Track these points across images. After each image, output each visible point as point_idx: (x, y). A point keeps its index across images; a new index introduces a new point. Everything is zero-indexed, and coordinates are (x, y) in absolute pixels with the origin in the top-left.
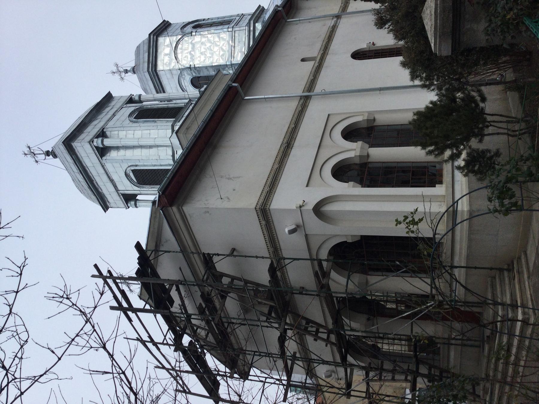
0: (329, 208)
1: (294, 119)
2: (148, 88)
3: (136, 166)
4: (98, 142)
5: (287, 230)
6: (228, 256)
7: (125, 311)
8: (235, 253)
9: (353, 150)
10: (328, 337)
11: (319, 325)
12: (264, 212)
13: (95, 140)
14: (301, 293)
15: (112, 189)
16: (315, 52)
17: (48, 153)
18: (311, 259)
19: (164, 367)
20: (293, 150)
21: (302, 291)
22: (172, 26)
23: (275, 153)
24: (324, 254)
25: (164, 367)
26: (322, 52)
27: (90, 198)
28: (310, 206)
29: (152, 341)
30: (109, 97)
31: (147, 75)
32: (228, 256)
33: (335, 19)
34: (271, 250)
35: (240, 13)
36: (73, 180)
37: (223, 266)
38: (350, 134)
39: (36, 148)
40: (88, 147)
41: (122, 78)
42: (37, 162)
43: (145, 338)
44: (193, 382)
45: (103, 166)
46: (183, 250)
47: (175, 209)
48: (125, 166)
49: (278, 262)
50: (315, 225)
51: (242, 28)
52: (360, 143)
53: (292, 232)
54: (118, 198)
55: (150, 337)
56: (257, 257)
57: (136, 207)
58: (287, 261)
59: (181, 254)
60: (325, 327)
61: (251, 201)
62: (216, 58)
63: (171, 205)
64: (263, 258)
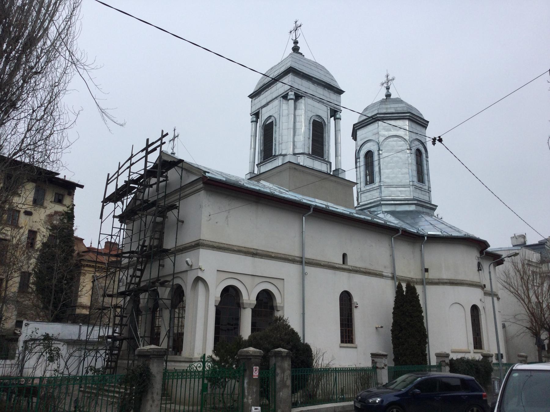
1: (279, 256)
3: (276, 125)
4: (291, 95)
5: (188, 259)
6: (178, 219)
7: (146, 149)
8: (180, 223)
9: (249, 297)
10: (133, 284)
11: (140, 277)
12: (197, 245)
13: (293, 93)
14: (160, 265)
15: (264, 103)
17: (296, 42)
18: (174, 274)
19: (119, 169)
20: (251, 258)
21: (162, 266)
22: (423, 130)
24: (177, 281)
25: (119, 169)
26: (351, 268)
27: (258, 84)
28: (200, 274)
29: (131, 165)
30: (340, 92)
32: (178, 219)
33: (390, 275)
34: (181, 248)
35: (432, 189)
36: (272, 68)
37: (172, 215)
41: (383, 84)
42: (291, 32)
43: (134, 160)
44: (111, 189)
45: (276, 98)
46: (182, 188)
47: (202, 185)
48: (276, 116)
49: (172, 253)
50: (191, 277)
51: (412, 193)
52: (255, 302)
54: (257, 108)
55: (133, 164)
56: (176, 239)
57: (252, 122)
58: (173, 258)
59: (179, 187)
60: (140, 281)
61: (206, 235)
62: (387, 171)
63: (203, 183)
64: (176, 242)
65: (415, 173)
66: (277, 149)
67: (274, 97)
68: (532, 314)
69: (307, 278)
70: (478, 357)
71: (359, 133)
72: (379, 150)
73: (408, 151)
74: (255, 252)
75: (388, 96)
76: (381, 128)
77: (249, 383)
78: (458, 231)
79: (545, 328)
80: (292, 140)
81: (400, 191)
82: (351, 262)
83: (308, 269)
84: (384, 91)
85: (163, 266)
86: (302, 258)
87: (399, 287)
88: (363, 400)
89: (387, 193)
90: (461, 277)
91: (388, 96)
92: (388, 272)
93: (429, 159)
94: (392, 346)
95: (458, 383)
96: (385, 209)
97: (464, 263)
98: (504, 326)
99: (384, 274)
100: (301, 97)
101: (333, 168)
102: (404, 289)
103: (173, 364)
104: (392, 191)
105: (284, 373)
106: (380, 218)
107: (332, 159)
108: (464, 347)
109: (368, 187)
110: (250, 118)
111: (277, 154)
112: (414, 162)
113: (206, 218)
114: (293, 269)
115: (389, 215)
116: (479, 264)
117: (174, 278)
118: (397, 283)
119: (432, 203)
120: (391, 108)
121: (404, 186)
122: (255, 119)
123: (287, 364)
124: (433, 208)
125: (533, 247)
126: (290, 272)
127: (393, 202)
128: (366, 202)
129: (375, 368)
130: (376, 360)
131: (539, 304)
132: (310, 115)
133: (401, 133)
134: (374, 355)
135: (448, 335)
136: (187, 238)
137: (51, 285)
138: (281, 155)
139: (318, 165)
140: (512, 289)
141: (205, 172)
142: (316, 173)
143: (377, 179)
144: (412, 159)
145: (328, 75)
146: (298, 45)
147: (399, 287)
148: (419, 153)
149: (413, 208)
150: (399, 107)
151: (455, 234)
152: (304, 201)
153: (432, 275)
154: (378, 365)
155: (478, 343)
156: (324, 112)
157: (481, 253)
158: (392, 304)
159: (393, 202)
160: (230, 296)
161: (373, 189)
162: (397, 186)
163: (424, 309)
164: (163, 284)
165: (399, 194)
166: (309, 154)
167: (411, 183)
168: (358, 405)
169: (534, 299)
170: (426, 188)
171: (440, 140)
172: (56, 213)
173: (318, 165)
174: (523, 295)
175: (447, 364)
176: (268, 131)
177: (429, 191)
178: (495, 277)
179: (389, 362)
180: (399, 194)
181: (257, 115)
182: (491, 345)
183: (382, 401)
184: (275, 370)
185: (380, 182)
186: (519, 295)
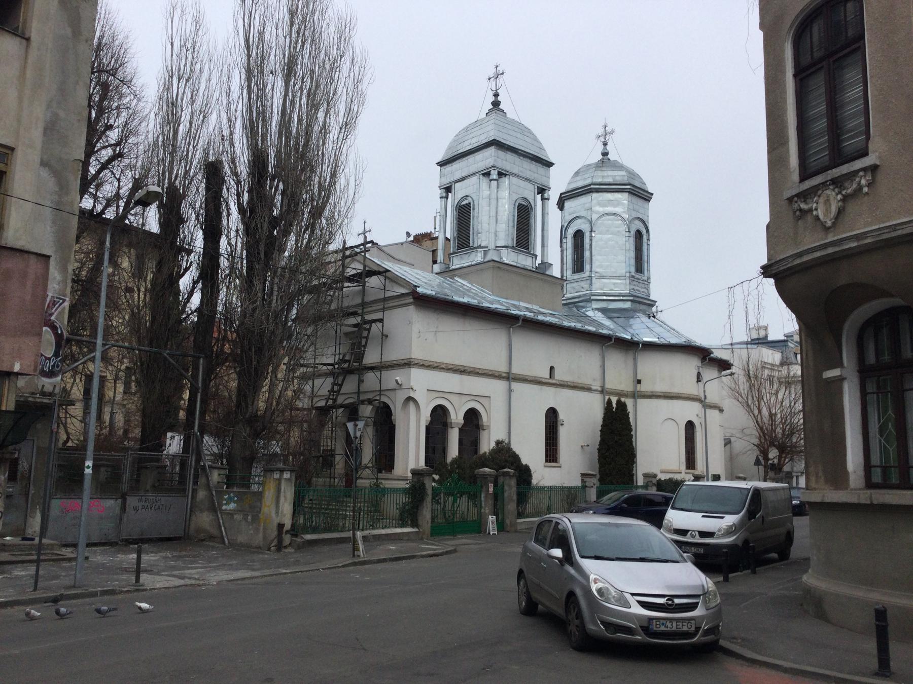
0: (412, 405)
2: (578, 178)
6: (383, 334)
9: (457, 417)
12: (408, 364)
16: (559, 376)
21: (361, 381)
22: (645, 203)
27: (449, 148)
30: (549, 164)
31: (588, 182)
33: (599, 389)
35: (652, 280)
36: (467, 129)
37: (375, 327)
40: (489, 162)
45: (474, 174)
46: (385, 299)
47: (412, 300)
50: (401, 396)
53: (397, 381)
54: (449, 181)
61: (417, 354)
62: (599, 257)
65: (633, 262)
66: (475, 241)
67: (472, 171)
68: (761, 428)
69: (513, 394)
71: (567, 204)
73: (627, 234)
74: (462, 369)
75: (605, 154)
76: (594, 202)
77: (486, 497)
79: (774, 446)
80: (493, 226)
81: (614, 284)
82: (559, 376)
83: (515, 386)
84: (600, 148)
87: (609, 402)
89: (599, 286)
90: (675, 390)
91: (605, 154)
92: (596, 386)
93: (651, 242)
94: (598, 465)
96: (595, 305)
97: (680, 373)
98: (728, 442)
99: (593, 387)
100: (506, 175)
101: (539, 261)
102: (614, 405)
105: (511, 489)
106: (593, 322)
107: (538, 251)
108: (674, 467)
109: (576, 276)
110: (438, 192)
111: (476, 245)
112: (633, 248)
113: (416, 335)
115: (600, 314)
116: (699, 375)
117: (380, 395)
118: (607, 398)
119: (652, 298)
121: (619, 278)
122: (444, 195)
123: (513, 482)
126: (497, 388)
127: (605, 298)
128: (572, 295)
129: (584, 487)
130: (585, 479)
132: (515, 197)
133: (618, 210)
134: (583, 475)
136: (394, 354)
138: (480, 247)
139: (524, 261)
140: (740, 399)
141: (416, 287)
143: (587, 267)
144: (631, 244)
145: (535, 143)
146: (499, 98)
148: (639, 235)
149: (628, 305)
150: (618, 176)
151: (674, 341)
153: (644, 387)
154: (587, 484)
156: (529, 192)
157: (703, 359)
158: (600, 421)
159: (605, 298)
160: (440, 414)
161: (582, 280)
162: (611, 278)
163: (633, 427)
164: (370, 402)
165: (612, 287)
166: (513, 247)
167: (628, 275)
169: (765, 412)
170: (645, 278)
173: (524, 261)
175: (654, 484)
176: (464, 213)
177: (648, 281)
178: (716, 387)
179: (595, 481)
180: (612, 287)
184: (503, 488)
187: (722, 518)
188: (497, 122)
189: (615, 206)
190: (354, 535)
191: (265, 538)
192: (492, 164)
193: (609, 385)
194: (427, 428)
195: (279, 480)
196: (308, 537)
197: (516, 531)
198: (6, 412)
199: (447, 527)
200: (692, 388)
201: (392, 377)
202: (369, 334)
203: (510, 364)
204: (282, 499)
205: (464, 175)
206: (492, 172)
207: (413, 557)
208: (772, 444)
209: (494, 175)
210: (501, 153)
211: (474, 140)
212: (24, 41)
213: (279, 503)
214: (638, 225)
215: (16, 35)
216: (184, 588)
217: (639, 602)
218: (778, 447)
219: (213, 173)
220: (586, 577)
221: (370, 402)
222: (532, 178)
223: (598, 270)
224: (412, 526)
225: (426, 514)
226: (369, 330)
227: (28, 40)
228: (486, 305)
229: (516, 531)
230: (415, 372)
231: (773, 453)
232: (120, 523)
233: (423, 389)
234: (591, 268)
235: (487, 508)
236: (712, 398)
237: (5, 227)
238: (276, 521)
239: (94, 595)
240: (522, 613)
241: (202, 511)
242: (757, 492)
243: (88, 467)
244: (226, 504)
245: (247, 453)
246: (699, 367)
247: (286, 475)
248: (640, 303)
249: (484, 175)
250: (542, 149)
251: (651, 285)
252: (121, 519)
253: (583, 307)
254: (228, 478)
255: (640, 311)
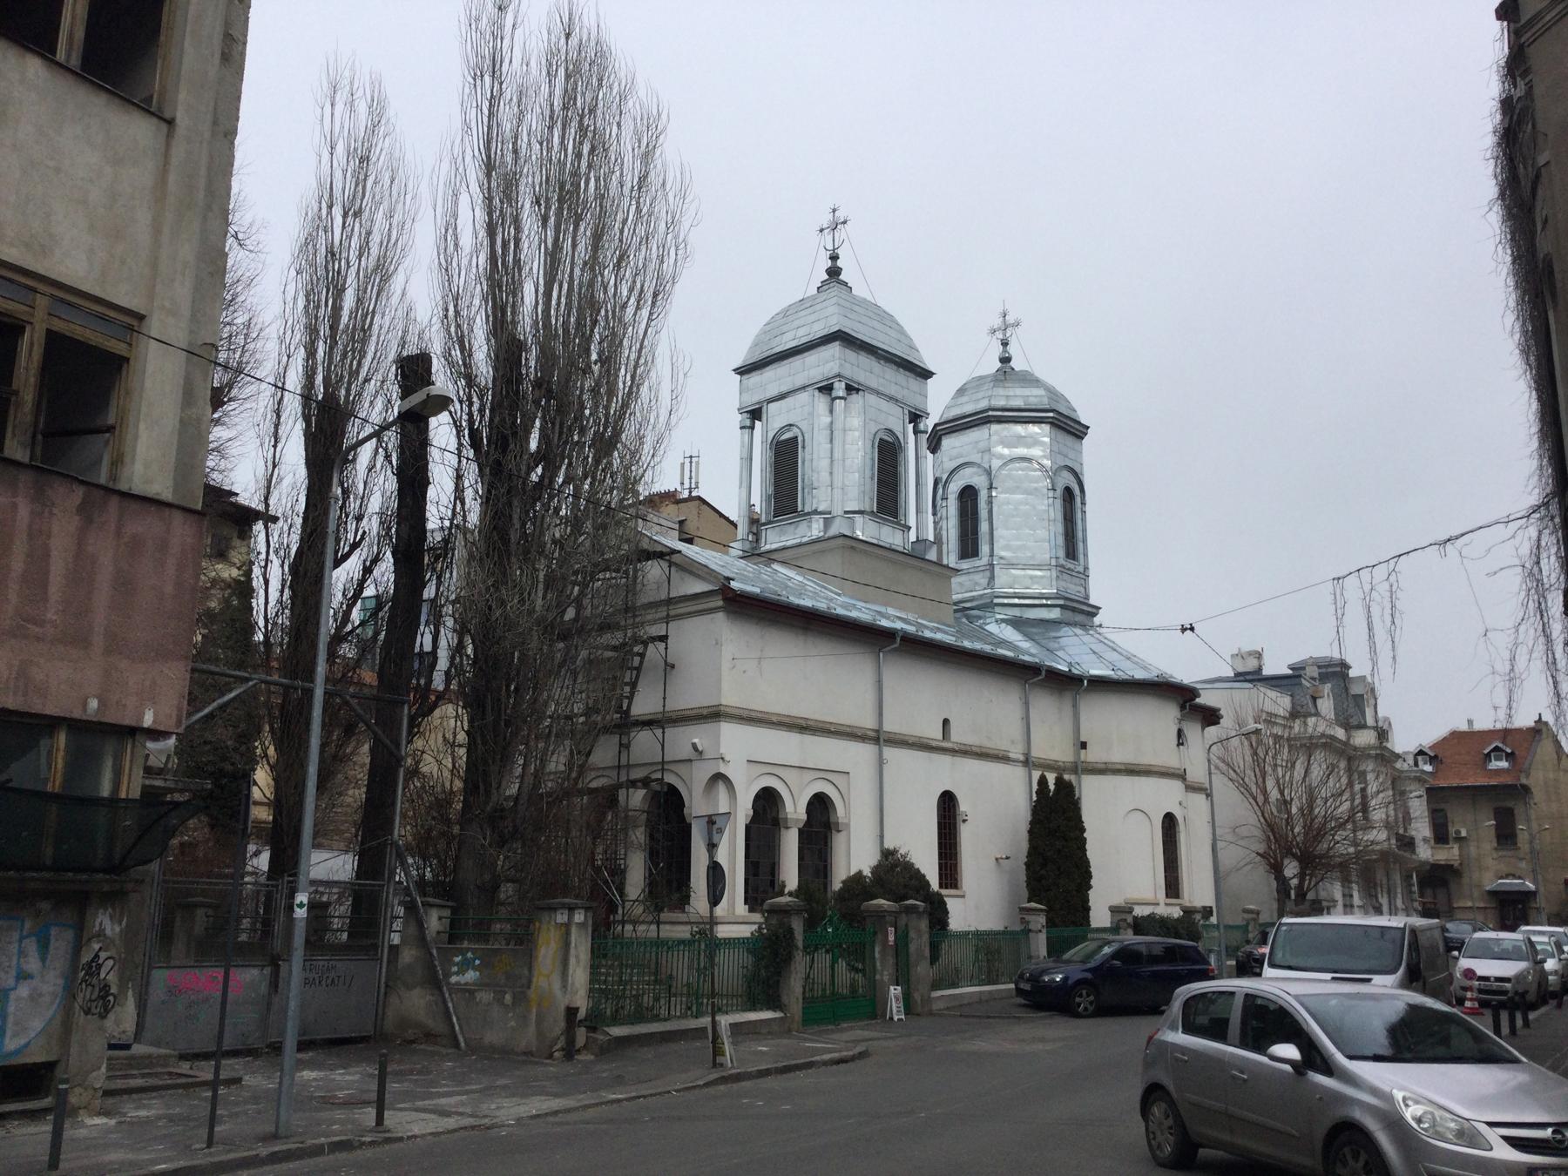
2: (965, 399)
9: (795, 809)
12: (715, 715)
13: (843, 385)
15: (773, 391)
16: (958, 736)
17: (834, 258)
18: (663, 762)
21: (625, 747)
23: (795, 713)
27: (756, 344)
30: (926, 374)
31: (983, 405)
33: (1022, 758)
34: (674, 716)
35: (1092, 572)
36: (785, 313)
37: (654, 652)
38: (820, 804)
39: (843, 235)
41: (994, 332)
45: (804, 388)
46: (670, 601)
47: (721, 603)
50: (701, 773)
52: (804, 817)
54: (756, 399)
61: (730, 698)
63: (724, 599)
65: (1061, 540)
66: (806, 502)
67: (799, 384)
70: (1176, 913)
71: (947, 443)
72: (991, 488)
73: (1051, 494)
74: (803, 723)
75: (1005, 360)
76: (994, 438)
77: (883, 952)
78: (1145, 668)
80: (838, 478)
81: (1032, 577)
82: (958, 736)
83: (890, 753)
85: (628, 746)
86: (877, 731)
87: (1043, 781)
88: (1035, 979)
89: (1006, 581)
91: (1005, 360)
92: (1017, 753)
93: (1088, 508)
95: (1157, 951)
100: (858, 390)
101: (913, 538)
102: (1052, 787)
103: (668, 927)
104: (1015, 577)
105: (920, 940)
107: (912, 522)
108: (1148, 895)
109: (965, 565)
110: (737, 419)
112: (1060, 516)
113: (727, 664)
114: (866, 751)
116: (1180, 733)
118: (1036, 775)
119: (1092, 602)
120: (1017, 396)
121: (1038, 567)
122: (748, 423)
124: (1093, 611)
125: (1275, 682)
126: (857, 756)
127: (1016, 601)
130: (1028, 918)
131: (1285, 803)
133: (1036, 452)
135: (1121, 874)
136: (686, 697)
137: (224, 759)
138: (816, 512)
139: (889, 536)
141: (729, 579)
142: (880, 552)
143: (984, 549)
144: (1057, 512)
146: (839, 263)
147: (1043, 781)
149: (1055, 614)
151: (1140, 675)
152: (884, 623)
153: (1093, 755)
154: (1031, 926)
155: (1173, 887)
156: (895, 420)
157: (1182, 707)
159: (1016, 601)
161: (977, 570)
162: (1025, 567)
167: (1053, 562)
168: (1027, 987)
169: (1274, 794)
171: (1192, 629)
172: (214, 582)
173: (889, 536)
174: (1254, 789)
176: (785, 455)
177: (1085, 575)
181: (755, 414)
182: (1199, 890)
183: (1065, 979)
185: (992, 555)
186: (1248, 790)
187: (1369, 980)
188: (842, 302)
189: (1029, 446)
190: (714, 1023)
191: (540, 1034)
192: (836, 371)
193: (1036, 753)
194: (747, 828)
195: (567, 926)
196: (617, 1031)
197: (931, 1014)
198: (127, 800)
199: (825, 1010)
200: (1167, 756)
201: (681, 740)
202: (641, 663)
203: (881, 714)
204: (572, 961)
205: (784, 389)
206: (836, 385)
207: (810, 1065)
208: (1288, 852)
209: (839, 389)
210: (851, 355)
211: (801, 332)
212: (164, 127)
213: (565, 969)
214: (1067, 479)
215: (153, 114)
216: (463, 1133)
217: (1505, 1138)
218: (1294, 856)
219: (414, 370)
220: (1389, 1098)
221: (645, 782)
222: (899, 397)
223: (1003, 554)
224: (774, 1009)
225: (794, 987)
226: (642, 655)
227: (170, 122)
228: (840, 611)
229: (931, 1014)
230: (727, 730)
231: (1291, 869)
232: (268, 1009)
233: (741, 761)
234: (992, 550)
235: (884, 972)
236: (1197, 773)
237: (127, 459)
238: (562, 1002)
239: (317, 1151)
240: (1162, 1164)
241: (409, 987)
242: (1413, 931)
243: (301, 905)
244: (457, 973)
245: (487, 877)
246: (1180, 721)
247: (579, 917)
248: (1074, 610)
249: (820, 389)
250: (913, 348)
251: (1091, 581)
252: (269, 1004)
253: (980, 618)
254: (453, 924)
255: (1074, 624)
